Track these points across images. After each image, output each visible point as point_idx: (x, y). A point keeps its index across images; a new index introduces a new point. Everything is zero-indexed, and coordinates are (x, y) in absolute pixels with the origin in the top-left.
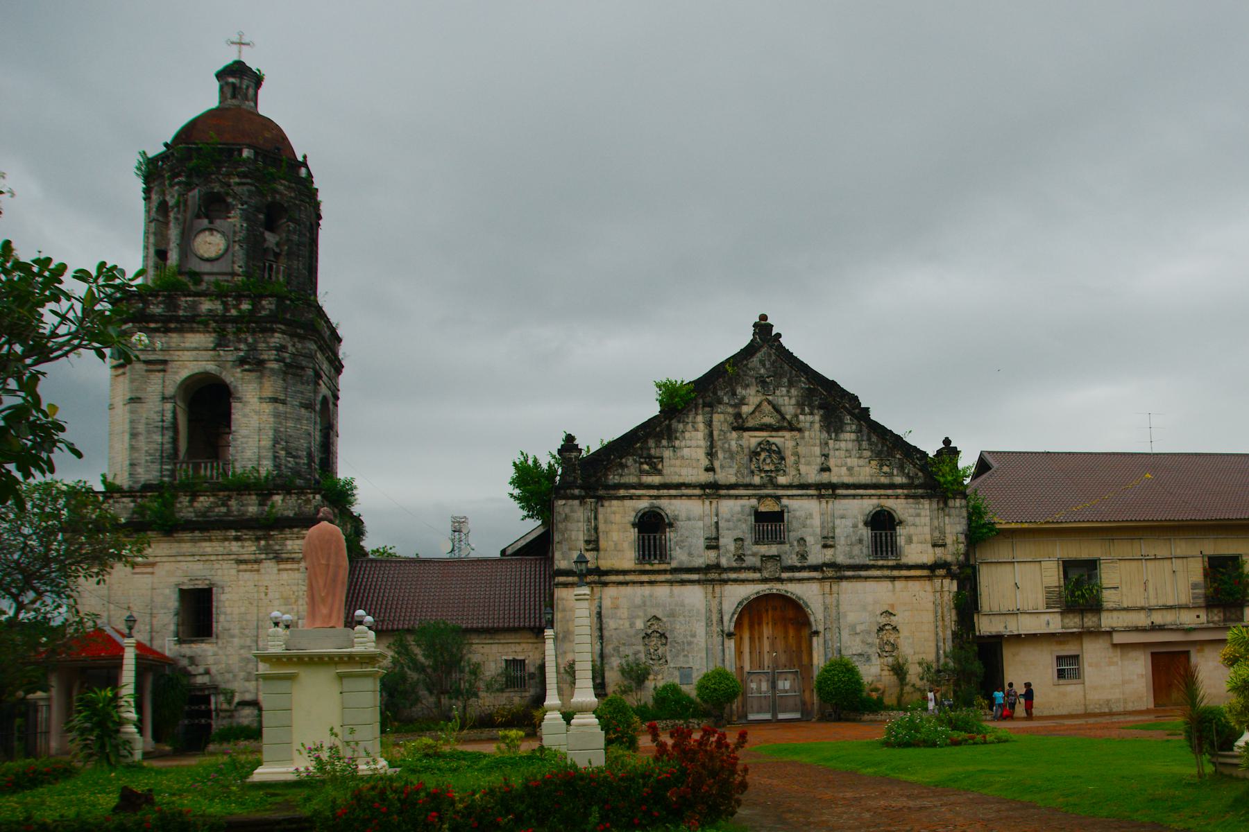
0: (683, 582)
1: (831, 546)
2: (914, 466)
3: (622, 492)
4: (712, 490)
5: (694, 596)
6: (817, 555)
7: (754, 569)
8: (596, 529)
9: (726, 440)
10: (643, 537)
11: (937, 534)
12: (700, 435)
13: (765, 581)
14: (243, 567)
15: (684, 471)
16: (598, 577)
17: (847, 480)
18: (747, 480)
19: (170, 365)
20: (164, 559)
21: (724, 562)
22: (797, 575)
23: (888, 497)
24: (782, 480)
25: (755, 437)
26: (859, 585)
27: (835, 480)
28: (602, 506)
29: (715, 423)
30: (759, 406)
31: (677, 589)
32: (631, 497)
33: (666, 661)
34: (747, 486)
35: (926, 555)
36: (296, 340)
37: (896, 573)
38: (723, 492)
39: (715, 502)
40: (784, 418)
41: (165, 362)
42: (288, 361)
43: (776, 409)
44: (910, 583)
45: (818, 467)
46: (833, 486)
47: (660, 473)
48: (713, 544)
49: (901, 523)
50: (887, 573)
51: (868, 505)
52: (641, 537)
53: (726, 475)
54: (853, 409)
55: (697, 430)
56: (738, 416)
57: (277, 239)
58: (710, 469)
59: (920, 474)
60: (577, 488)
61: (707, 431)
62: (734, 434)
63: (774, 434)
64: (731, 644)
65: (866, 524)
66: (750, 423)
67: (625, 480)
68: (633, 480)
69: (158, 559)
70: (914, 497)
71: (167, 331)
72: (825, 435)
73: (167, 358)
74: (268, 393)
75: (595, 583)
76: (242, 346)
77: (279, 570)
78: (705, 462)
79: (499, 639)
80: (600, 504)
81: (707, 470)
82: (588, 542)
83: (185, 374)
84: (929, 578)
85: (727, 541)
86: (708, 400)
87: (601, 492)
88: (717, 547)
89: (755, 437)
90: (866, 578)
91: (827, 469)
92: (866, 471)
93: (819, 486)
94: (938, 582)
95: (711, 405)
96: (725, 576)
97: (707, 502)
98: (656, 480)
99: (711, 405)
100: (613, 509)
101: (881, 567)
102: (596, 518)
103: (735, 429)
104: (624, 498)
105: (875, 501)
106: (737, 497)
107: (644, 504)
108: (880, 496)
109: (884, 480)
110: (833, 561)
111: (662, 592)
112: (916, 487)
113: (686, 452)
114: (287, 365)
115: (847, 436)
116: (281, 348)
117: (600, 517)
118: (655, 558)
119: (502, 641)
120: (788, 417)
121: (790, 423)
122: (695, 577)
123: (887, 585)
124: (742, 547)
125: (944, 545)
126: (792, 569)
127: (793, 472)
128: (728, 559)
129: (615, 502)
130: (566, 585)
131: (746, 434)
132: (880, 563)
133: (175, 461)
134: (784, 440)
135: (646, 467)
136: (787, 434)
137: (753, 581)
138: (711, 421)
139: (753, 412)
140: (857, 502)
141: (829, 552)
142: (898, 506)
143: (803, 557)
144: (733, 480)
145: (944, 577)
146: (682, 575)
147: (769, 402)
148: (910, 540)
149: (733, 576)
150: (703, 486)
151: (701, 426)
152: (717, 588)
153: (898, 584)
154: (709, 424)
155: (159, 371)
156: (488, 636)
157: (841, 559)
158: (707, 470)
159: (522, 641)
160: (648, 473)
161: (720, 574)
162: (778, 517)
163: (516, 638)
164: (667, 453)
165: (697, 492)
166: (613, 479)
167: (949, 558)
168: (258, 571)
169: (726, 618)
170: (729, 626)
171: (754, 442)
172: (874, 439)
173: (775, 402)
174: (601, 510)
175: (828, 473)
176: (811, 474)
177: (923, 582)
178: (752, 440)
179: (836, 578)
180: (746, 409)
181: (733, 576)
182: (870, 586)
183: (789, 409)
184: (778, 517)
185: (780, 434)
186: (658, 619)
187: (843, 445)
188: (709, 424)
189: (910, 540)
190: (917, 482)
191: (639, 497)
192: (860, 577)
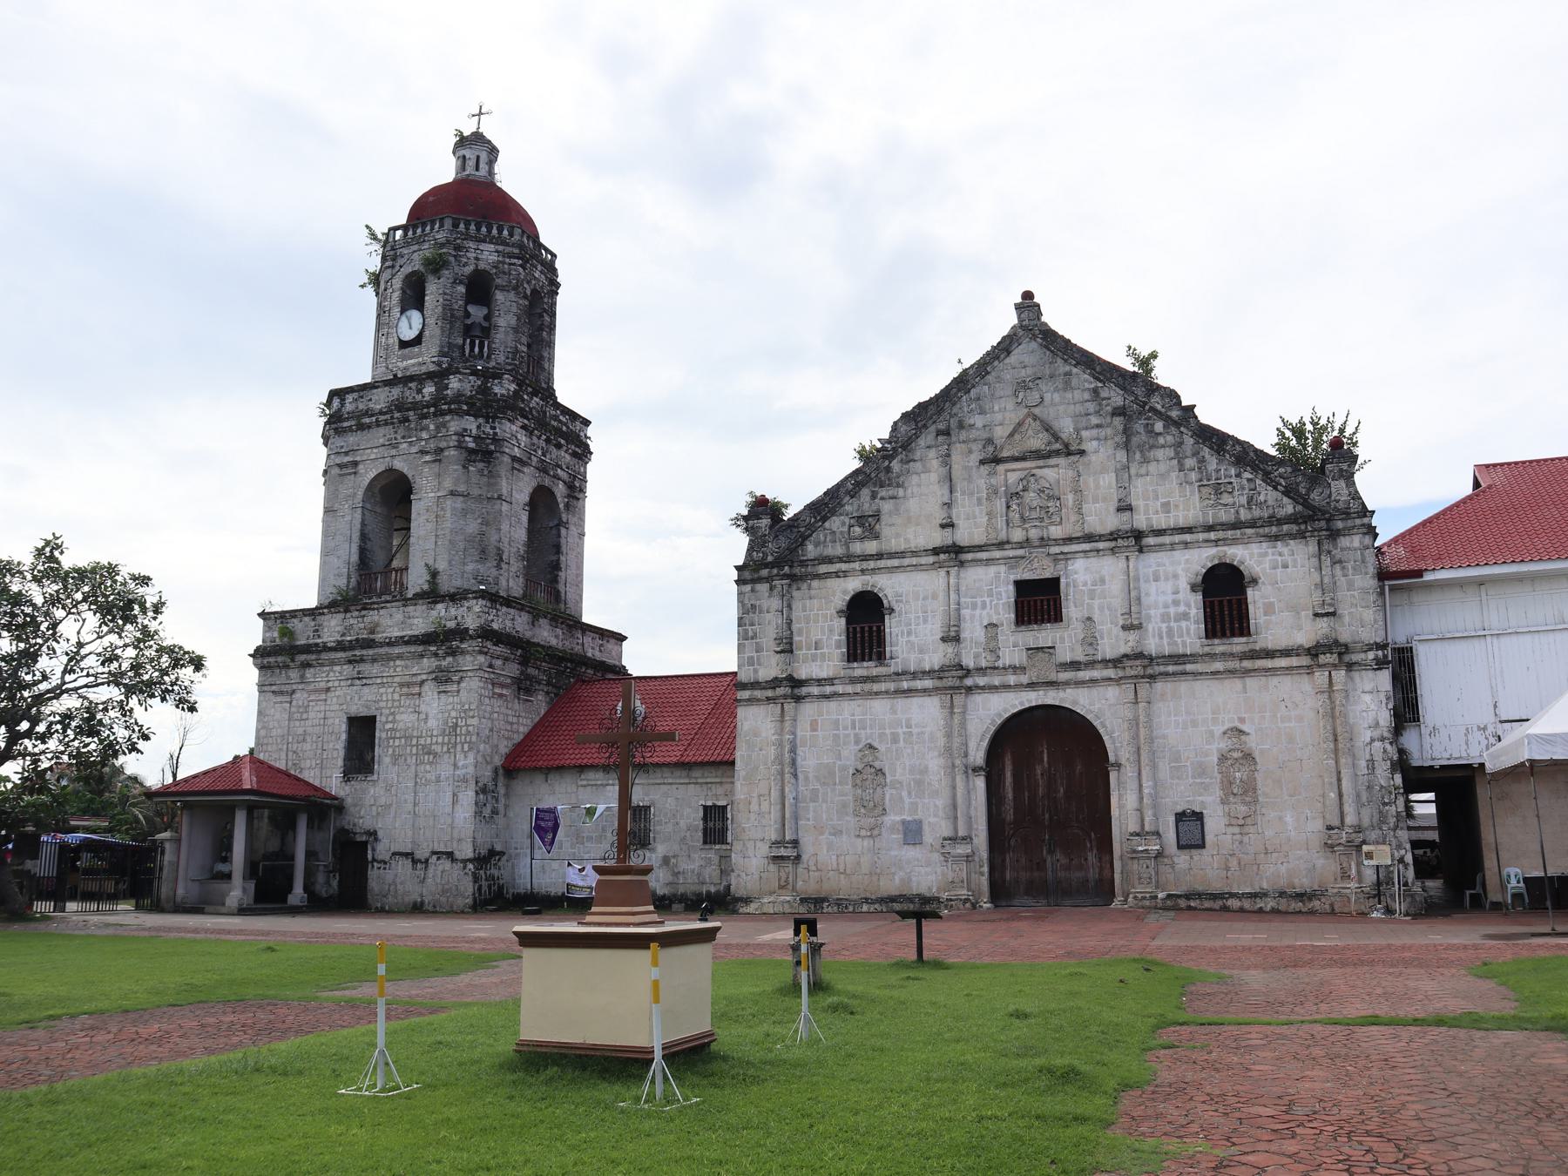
0: (909, 692)
1: (1139, 627)
2: (1275, 488)
3: (823, 569)
4: (954, 554)
5: (926, 712)
6: (1113, 643)
7: (1015, 669)
8: (790, 623)
9: (969, 479)
10: (855, 629)
11: (1317, 595)
12: (934, 477)
13: (1032, 686)
14: (405, 690)
15: (910, 532)
16: (792, 688)
17: (1161, 521)
18: (1003, 536)
19: (361, 467)
20: (336, 684)
21: (968, 662)
22: (1085, 675)
23: (1234, 542)
24: (1056, 532)
25: (1014, 470)
26: (1184, 686)
27: (1140, 522)
28: (799, 589)
29: (957, 458)
30: (1020, 424)
31: (901, 703)
32: (837, 575)
33: (884, 809)
34: (1001, 545)
35: (1307, 633)
36: (481, 420)
37: (1247, 664)
38: (969, 556)
39: (953, 571)
40: (1056, 438)
41: (355, 464)
42: (472, 445)
43: (1048, 428)
44: (1274, 681)
45: (1113, 505)
46: (1138, 535)
47: (877, 537)
48: (952, 637)
49: (1254, 581)
50: (1232, 664)
51: (1200, 559)
52: (851, 630)
53: (967, 533)
54: (1170, 408)
55: (927, 471)
56: (990, 441)
57: (485, 311)
58: (948, 525)
59: (1286, 500)
60: (766, 566)
61: (943, 471)
62: (985, 469)
63: (1041, 463)
64: (980, 783)
65: (1194, 588)
66: (1005, 454)
67: (830, 551)
68: (839, 550)
69: (330, 684)
70: (1276, 538)
71: (362, 427)
72: (1121, 455)
73: (358, 459)
74: (448, 484)
75: (785, 697)
76: (425, 435)
77: (439, 692)
78: (939, 516)
79: (696, 778)
80: (795, 587)
81: (943, 526)
82: (779, 640)
83: (372, 475)
84: (1309, 670)
85: (973, 631)
86: (941, 426)
87: (797, 570)
88: (957, 639)
89: (1014, 470)
90: (1196, 675)
91: (1125, 508)
92: (1189, 507)
93: (1113, 536)
94: (1321, 677)
95: (946, 433)
96: (969, 682)
97: (942, 572)
98: (871, 547)
99: (946, 433)
100: (813, 592)
101: (1225, 656)
102: (789, 606)
103: (982, 462)
104: (828, 575)
105: (1212, 551)
106: (989, 562)
107: (854, 585)
108: (1216, 542)
109: (1225, 516)
110: (1139, 650)
111: (879, 707)
112: (1280, 522)
113: (912, 505)
114: (471, 451)
115: (1160, 453)
116: (461, 434)
117: (797, 605)
118: (870, 660)
119: (700, 781)
120: (1064, 436)
121: (1067, 445)
122: (928, 683)
123: (1237, 684)
124: (995, 638)
125: (1333, 614)
126: (1075, 665)
127: (1073, 518)
128: (976, 656)
129: (815, 583)
130: (751, 701)
131: (1001, 468)
132: (1219, 649)
133: (362, 572)
134: (1055, 473)
135: (857, 530)
136: (1061, 461)
137: (1006, 687)
138: (948, 455)
139: (1011, 435)
140: (1181, 556)
141: (1132, 636)
142: (1249, 556)
143: (1091, 641)
144: (979, 537)
145: (1335, 666)
146: (906, 684)
147: (1035, 418)
148: (1269, 609)
149: (981, 681)
150: (936, 551)
151: (935, 463)
152: (958, 699)
153: (1251, 682)
154: (946, 459)
155: (350, 474)
156: (684, 773)
157: (1152, 646)
158: (943, 526)
159: (724, 780)
160: (862, 539)
161: (961, 678)
162: (1052, 586)
163: (716, 777)
164: (886, 507)
165: (931, 559)
166: (811, 550)
167: (1345, 636)
168: (420, 694)
169: (972, 745)
170: (978, 756)
171: (1013, 478)
172: (1206, 452)
173: (1044, 416)
174: (795, 594)
175: (1128, 514)
176: (1102, 518)
177: (1296, 678)
178: (1011, 475)
179: (1143, 677)
180: (1000, 433)
181: (981, 681)
182: (1202, 688)
183: (1066, 427)
184: (1052, 586)
185: (1052, 461)
186: (871, 747)
187: (1152, 467)
188: (946, 459)
189: (1269, 609)
190: (1281, 513)
191: (845, 574)
192: (1185, 673)
